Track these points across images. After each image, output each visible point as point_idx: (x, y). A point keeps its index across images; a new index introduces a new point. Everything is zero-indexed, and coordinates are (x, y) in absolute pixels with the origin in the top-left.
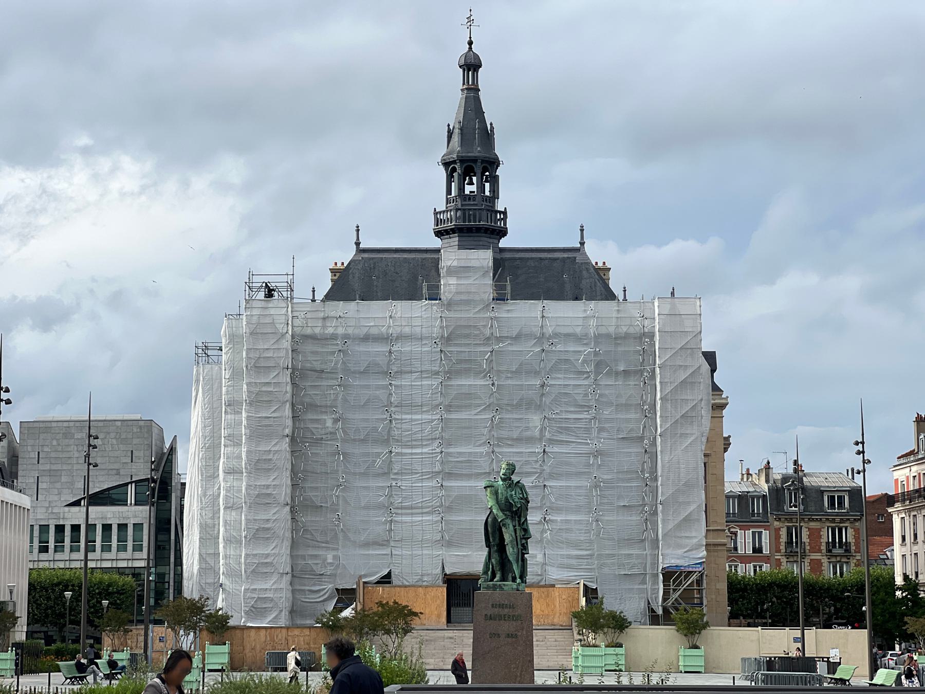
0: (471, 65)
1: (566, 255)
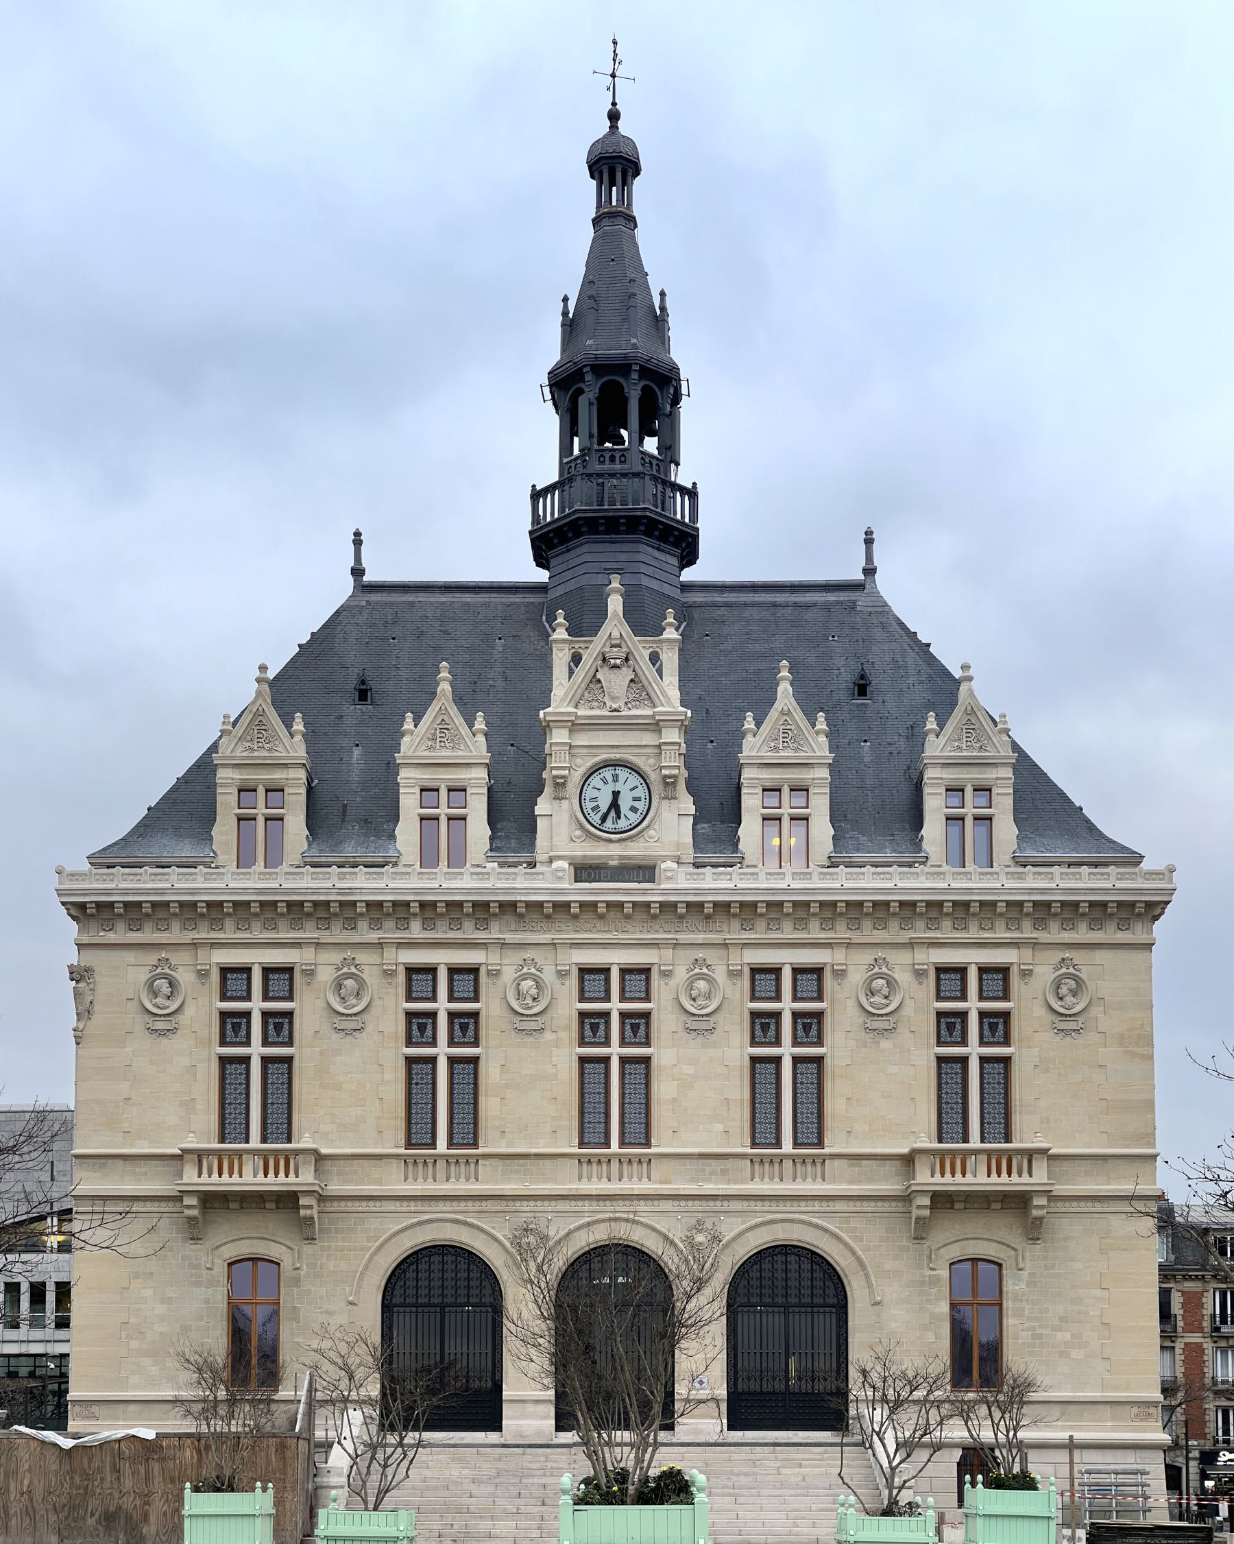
1: (831, 597)
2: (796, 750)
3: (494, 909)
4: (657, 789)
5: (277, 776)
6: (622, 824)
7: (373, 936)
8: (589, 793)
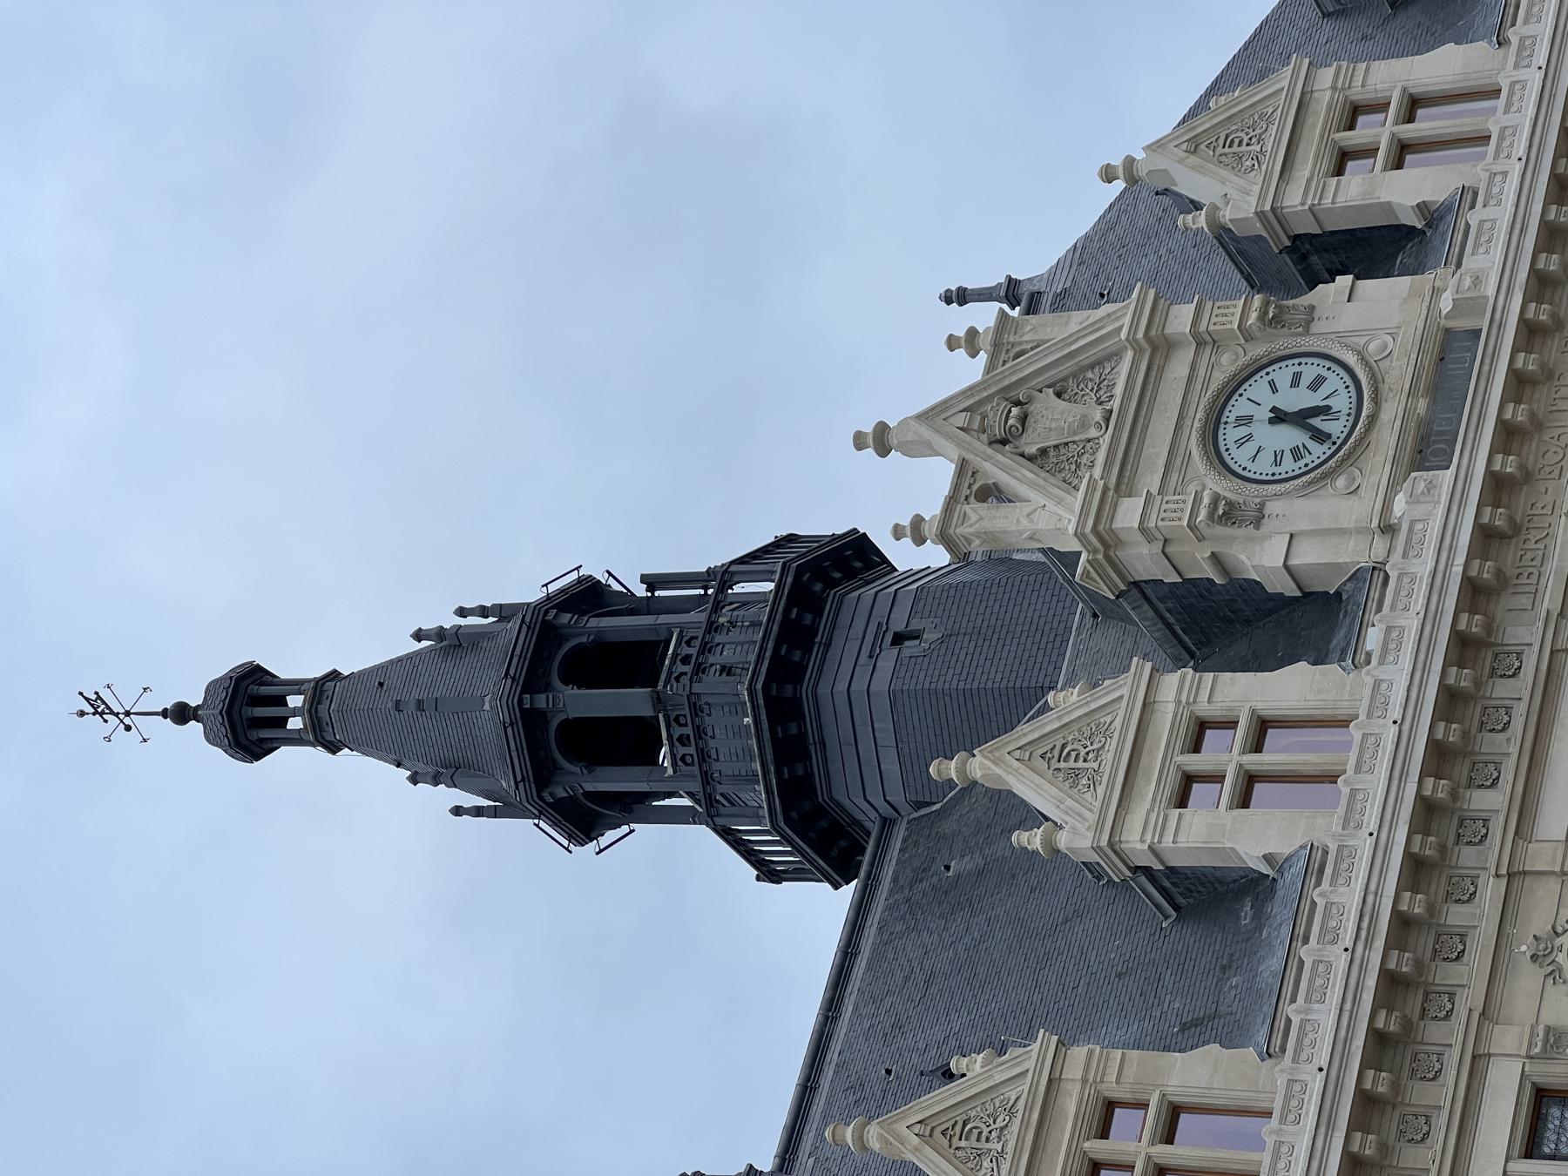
0: (248, 713)
2: (1269, 122)
3: (1473, 624)
4: (1284, 342)
5: (1070, 1105)
6: (1342, 403)
7: (1491, 891)
8: (1264, 467)
